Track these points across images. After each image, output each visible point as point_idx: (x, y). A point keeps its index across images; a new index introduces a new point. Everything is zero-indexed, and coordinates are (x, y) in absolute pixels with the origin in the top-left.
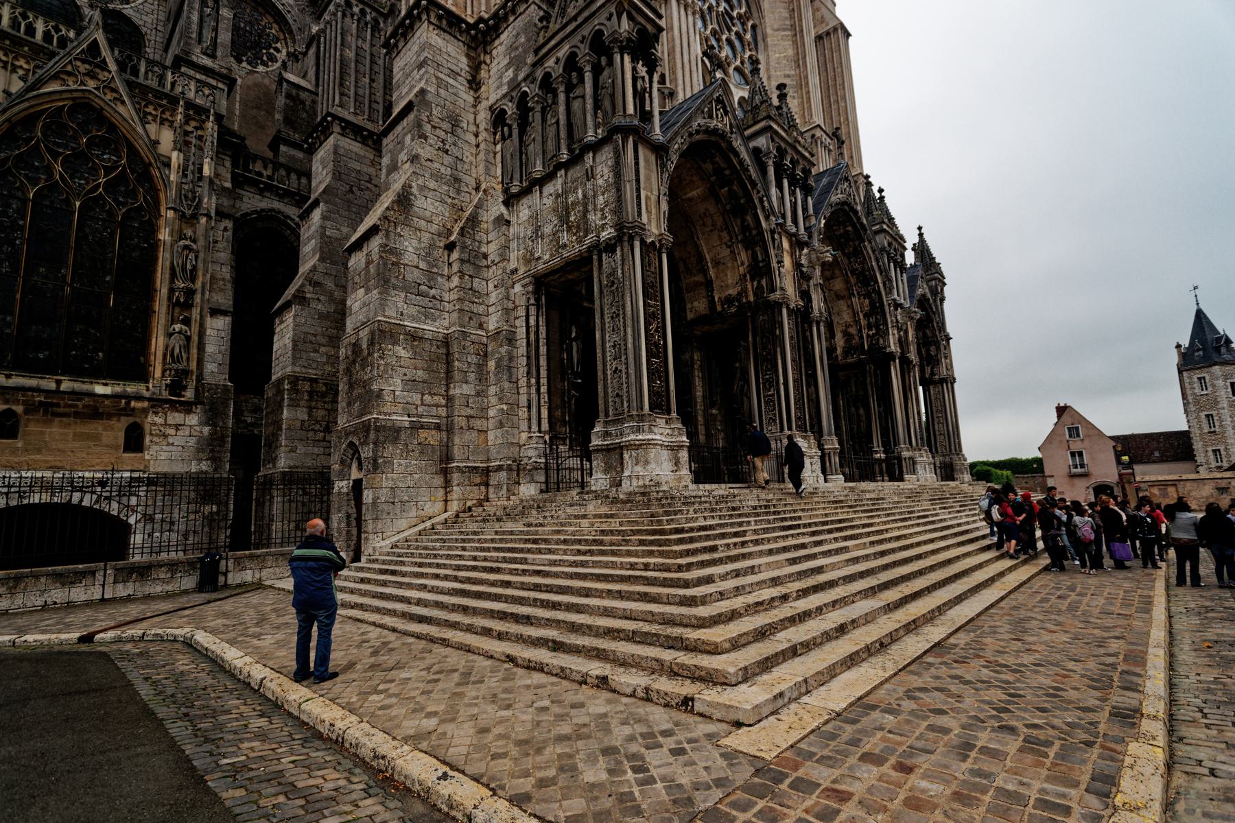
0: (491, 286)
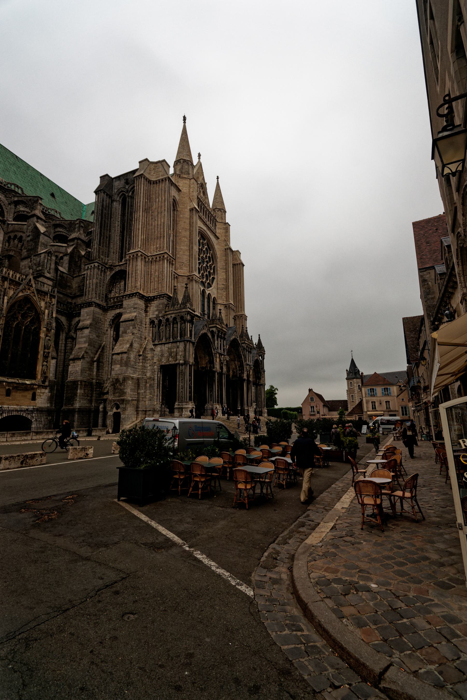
0: (148, 365)
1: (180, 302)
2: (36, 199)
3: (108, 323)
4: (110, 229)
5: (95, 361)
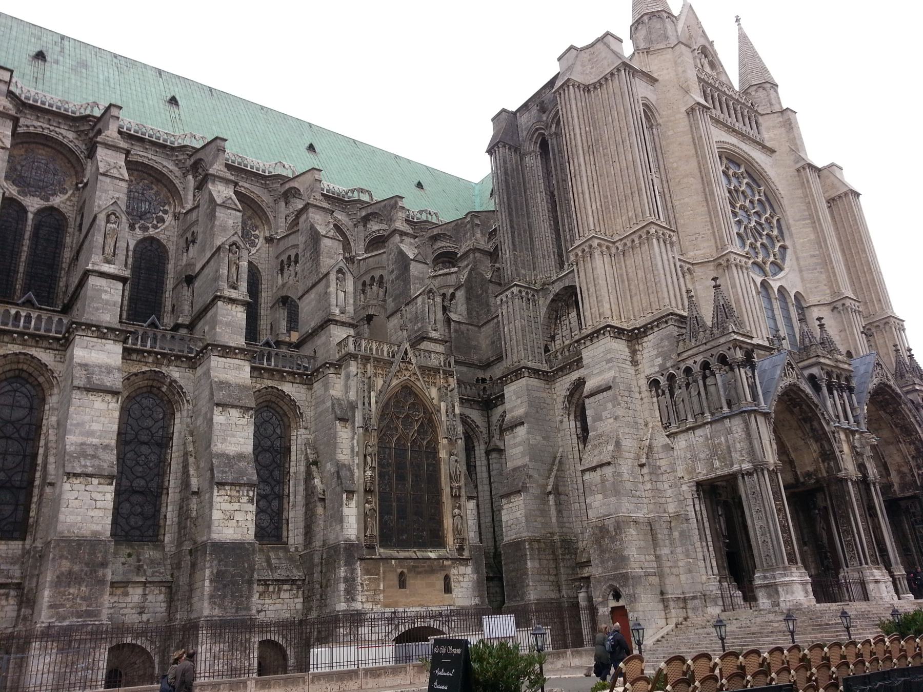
0: (666, 486)
1: (709, 324)
2: (393, 201)
3: (560, 406)
4: (528, 213)
5: (550, 493)
